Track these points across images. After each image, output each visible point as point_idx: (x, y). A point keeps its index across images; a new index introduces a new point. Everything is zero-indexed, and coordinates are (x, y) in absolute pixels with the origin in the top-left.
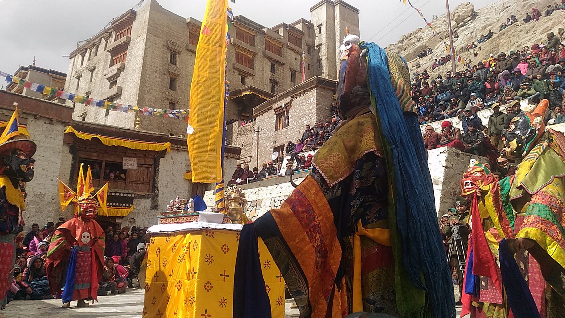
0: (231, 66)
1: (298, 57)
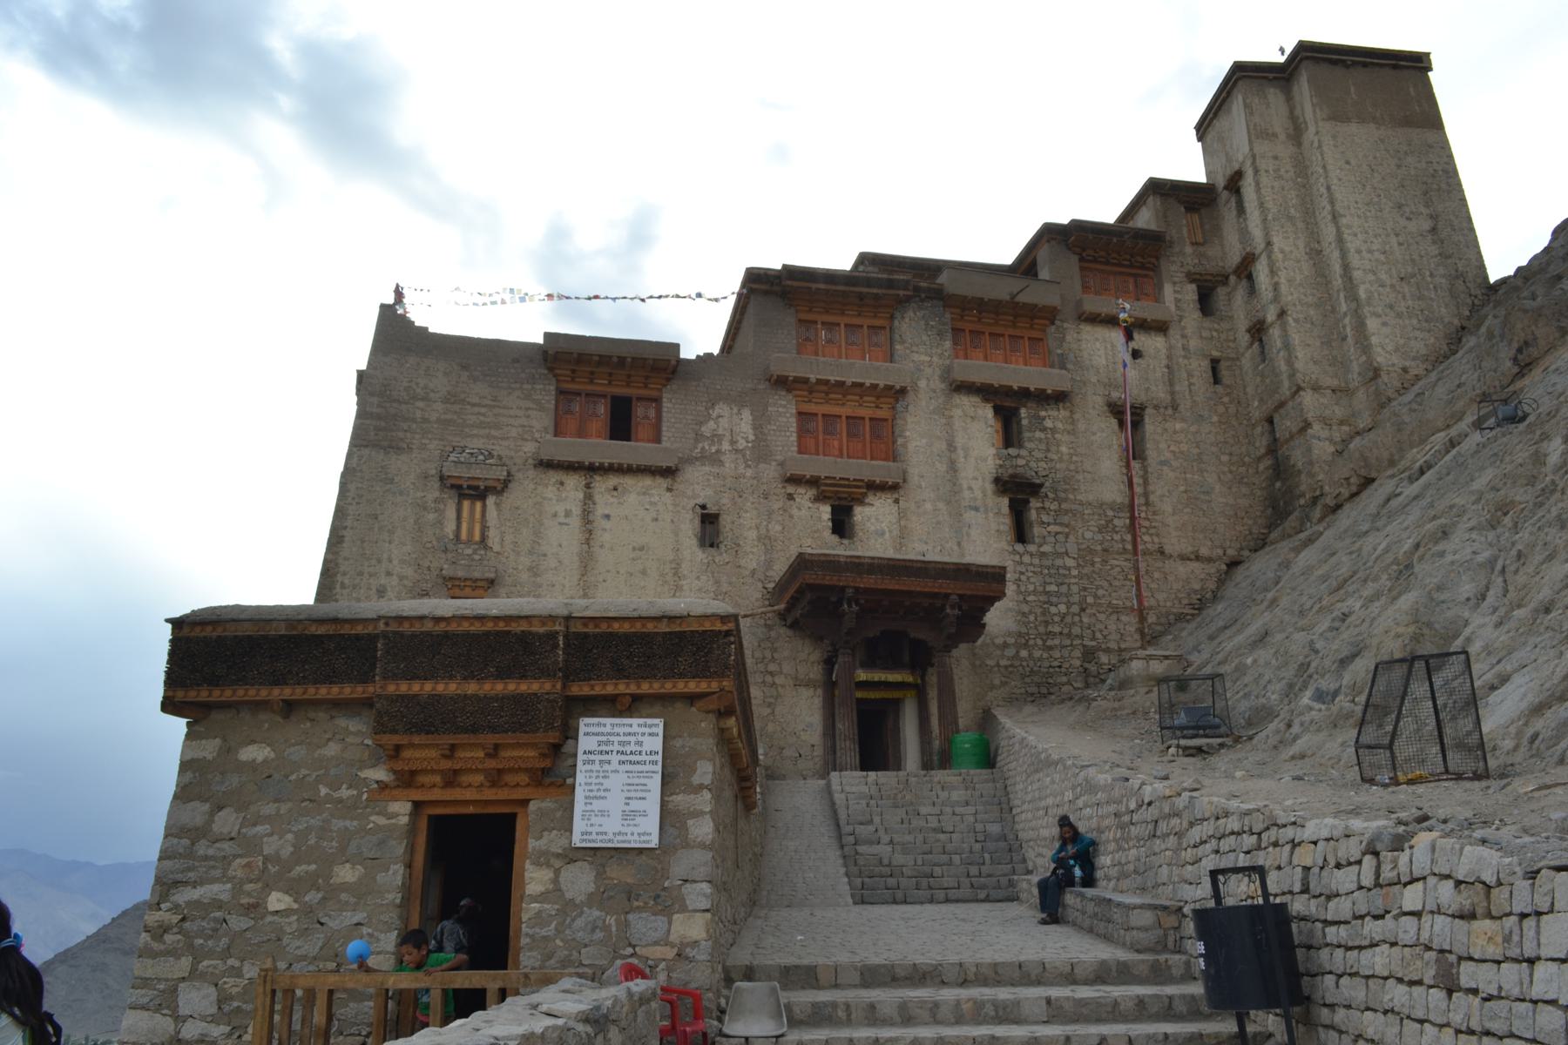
0: (770, 472)
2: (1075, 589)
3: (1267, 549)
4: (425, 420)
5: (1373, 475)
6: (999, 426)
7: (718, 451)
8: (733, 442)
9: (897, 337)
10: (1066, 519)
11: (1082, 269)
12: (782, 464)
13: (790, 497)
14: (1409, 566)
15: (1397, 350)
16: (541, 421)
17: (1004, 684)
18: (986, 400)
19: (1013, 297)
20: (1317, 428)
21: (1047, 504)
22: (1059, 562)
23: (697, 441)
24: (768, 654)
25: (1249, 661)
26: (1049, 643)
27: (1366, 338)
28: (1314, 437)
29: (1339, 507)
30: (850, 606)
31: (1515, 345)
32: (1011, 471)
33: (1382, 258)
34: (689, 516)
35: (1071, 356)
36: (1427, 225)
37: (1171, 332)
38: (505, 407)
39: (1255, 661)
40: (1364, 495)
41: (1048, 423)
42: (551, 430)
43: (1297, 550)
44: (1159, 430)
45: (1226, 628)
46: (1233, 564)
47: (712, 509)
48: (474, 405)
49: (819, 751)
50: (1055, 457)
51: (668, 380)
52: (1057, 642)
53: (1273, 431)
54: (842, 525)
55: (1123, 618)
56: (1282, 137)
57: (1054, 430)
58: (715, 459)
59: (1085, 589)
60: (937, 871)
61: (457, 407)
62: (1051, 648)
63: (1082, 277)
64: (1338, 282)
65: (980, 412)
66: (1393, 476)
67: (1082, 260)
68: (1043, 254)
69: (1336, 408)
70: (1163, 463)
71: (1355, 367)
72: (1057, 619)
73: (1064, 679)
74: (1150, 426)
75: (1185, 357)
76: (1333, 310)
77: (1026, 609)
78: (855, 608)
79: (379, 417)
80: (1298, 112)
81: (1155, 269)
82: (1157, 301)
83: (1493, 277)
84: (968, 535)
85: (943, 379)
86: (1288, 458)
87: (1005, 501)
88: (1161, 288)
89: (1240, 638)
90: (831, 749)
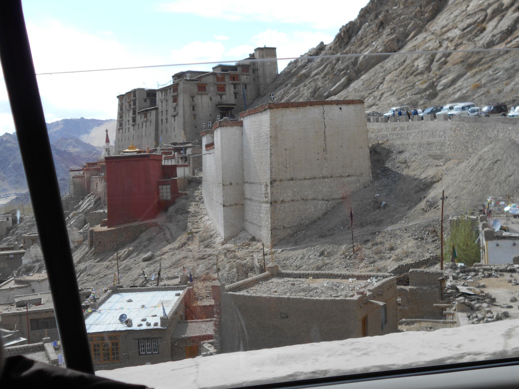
1: (248, 77)
54: (221, 98)
74: (248, 86)
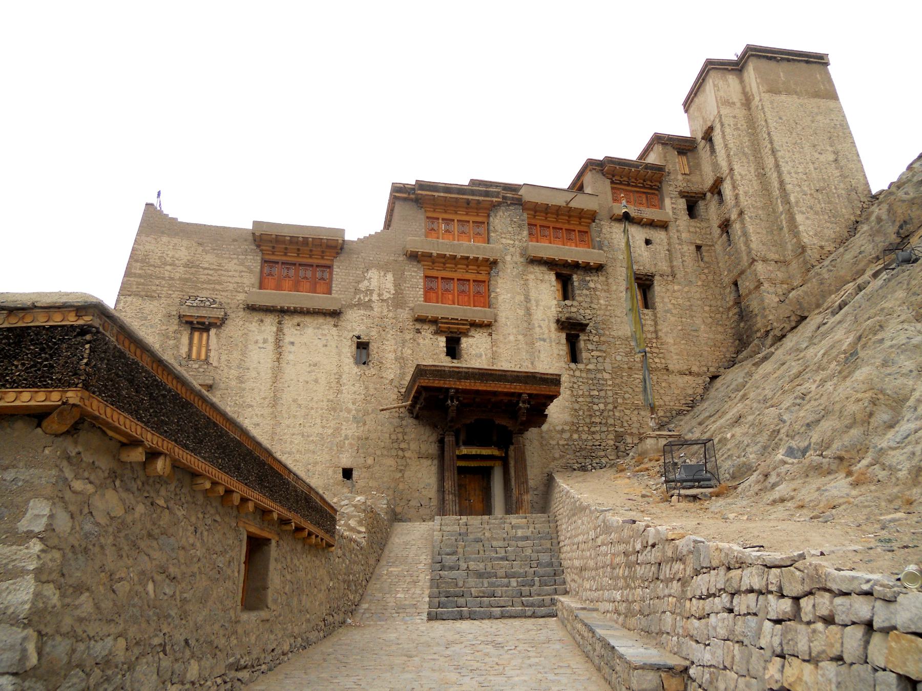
0: (405, 314)
1: (658, 236)
2: (610, 393)
3: (736, 366)
4: (171, 279)
5: (806, 314)
6: (560, 287)
7: (370, 300)
8: (379, 295)
9: (491, 228)
10: (604, 347)
11: (613, 188)
12: (412, 309)
13: (418, 331)
14: (854, 353)
15: (816, 235)
16: (250, 280)
17: (562, 457)
18: (551, 270)
19: (568, 203)
20: (766, 285)
21: (591, 338)
22: (599, 376)
23: (355, 293)
24: (400, 436)
25: (729, 436)
26: (593, 429)
27: (796, 227)
28: (764, 291)
29: (784, 336)
30: (452, 401)
31: (898, 224)
32: (567, 315)
33: (804, 177)
34: (349, 343)
35: (606, 242)
36: (832, 157)
37: (670, 228)
38: (226, 271)
39: (733, 436)
40: (800, 327)
41: (592, 285)
42: (257, 285)
43: (757, 365)
44: (664, 290)
45: (710, 416)
46: (714, 378)
47: (364, 339)
48: (206, 269)
49: (434, 502)
50: (596, 307)
51: (338, 253)
52: (598, 429)
53: (738, 290)
54: (453, 350)
55: (642, 413)
56: (738, 105)
57: (595, 289)
58: (368, 306)
59: (617, 394)
60: (499, 591)
61: (193, 270)
62: (594, 433)
63: (613, 194)
64: (776, 193)
65: (546, 277)
66: (820, 313)
67: (612, 182)
68: (588, 179)
69: (778, 273)
70: (667, 311)
71: (789, 247)
72: (598, 413)
73: (603, 453)
74: (658, 288)
75: (679, 244)
76: (774, 211)
77: (577, 406)
78: (456, 403)
79: (140, 276)
80: (748, 89)
81: (659, 189)
82: (660, 208)
83: (874, 192)
84: (539, 357)
85: (522, 255)
86: (748, 306)
87: (564, 335)
88: (662, 200)
89: (722, 421)
90: (442, 501)
